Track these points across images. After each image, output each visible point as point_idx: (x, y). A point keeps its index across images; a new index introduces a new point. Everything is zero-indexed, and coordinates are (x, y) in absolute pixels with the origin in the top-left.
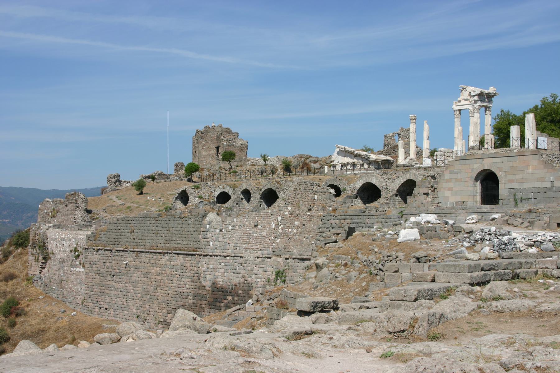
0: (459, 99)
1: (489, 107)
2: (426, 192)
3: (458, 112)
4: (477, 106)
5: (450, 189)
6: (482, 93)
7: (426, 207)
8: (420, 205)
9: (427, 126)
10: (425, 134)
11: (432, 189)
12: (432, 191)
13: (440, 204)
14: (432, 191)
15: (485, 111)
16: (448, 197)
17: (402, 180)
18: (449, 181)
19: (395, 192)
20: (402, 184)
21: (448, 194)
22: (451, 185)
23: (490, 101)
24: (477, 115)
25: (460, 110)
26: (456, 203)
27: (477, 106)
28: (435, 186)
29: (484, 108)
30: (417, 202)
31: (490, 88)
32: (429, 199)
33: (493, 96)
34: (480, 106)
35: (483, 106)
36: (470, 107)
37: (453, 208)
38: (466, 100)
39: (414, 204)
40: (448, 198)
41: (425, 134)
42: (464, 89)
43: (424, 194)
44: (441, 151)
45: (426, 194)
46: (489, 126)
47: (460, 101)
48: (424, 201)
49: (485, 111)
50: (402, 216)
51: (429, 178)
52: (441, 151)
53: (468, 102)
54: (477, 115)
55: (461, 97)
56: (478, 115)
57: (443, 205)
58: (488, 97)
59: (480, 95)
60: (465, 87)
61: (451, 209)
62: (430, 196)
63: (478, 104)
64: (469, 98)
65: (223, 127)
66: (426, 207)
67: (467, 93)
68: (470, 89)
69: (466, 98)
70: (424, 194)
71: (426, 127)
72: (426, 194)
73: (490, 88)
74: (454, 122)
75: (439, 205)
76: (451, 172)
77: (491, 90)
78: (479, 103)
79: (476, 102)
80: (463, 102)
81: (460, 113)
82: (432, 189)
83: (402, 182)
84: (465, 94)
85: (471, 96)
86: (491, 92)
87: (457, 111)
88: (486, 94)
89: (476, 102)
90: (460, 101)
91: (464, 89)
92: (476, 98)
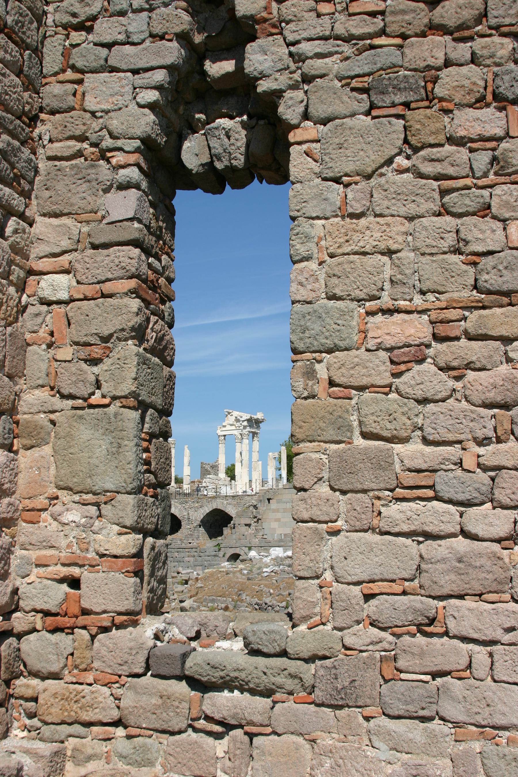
0: (224, 424)
1: (257, 434)
2: (248, 523)
3: (223, 438)
4: (245, 431)
5: (278, 520)
7: (248, 539)
8: (242, 537)
9: (188, 451)
10: (186, 460)
11: (255, 520)
12: (255, 522)
13: (265, 537)
14: (255, 522)
15: (253, 438)
16: (275, 529)
17: (207, 509)
18: (277, 511)
19: (198, 523)
20: (207, 514)
21: (274, 525)
22: (279, 515)
23: (258, 427)
24: (246, 441)
25: (225, 436)
26: (285, 535)
27: (245, 431)
28: (259, 517)
29: (251, 434)
30: (238, 534)
32: (251, 531)
33: (261, 422)
34: (249, 432)
35: (252, 432)
36: (236, 433)
37: (281, 540)
38: (231, 425)
39: (234, 536)
40: (274, 529)
41: (186, 460)
42: (229, 413)
43: (246, 525)
45: (249, 525)
46: (257, 453)
47: (224, 426)
48: (246, 533)
49: (253, 438)
50: (219, 550)
51: (251, 508)
53: (233, 428)
57: (269, 538)
58: (256, 423)
59: (249, 420)
60: (231, 411)
61: (279, 542)
62: (252, 527)
64: (235, 423)
66: (248, 539)
68: (236, 414)
69: (232, 423)
70: (246, 525)
71: (187, 452)
72: (249, 525)
75: (264, 537)
76: (278, 502)
77: (259, 416)
78: (248, 429)
79: (245, 427)
80: (229, 427)
81: (225, 439)
82: (255, 520)
83: (208, 511)
84: (231, 419)
85: (237, 420)
89: (245, 427)
90: (224, 426)
92: (245, 423)
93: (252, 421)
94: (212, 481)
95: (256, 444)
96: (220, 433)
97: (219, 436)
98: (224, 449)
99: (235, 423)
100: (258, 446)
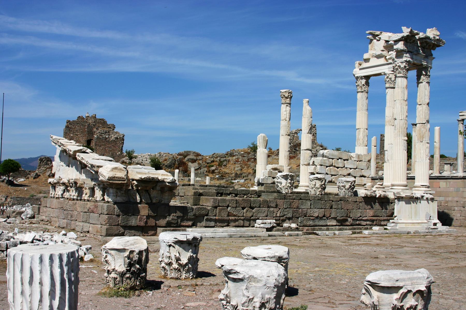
0: (366, 56)
3: (364, 81)
6: (412, 35)
15: (419, 77)
23: (429, 56)
25: (367, 78)
31: (428, 30)
36: (387, 70)
38: (378, 57)
42: (375, 36)
44: (323, 156)
46: (425, 107)
47: (367, 60)
49: (419, 77)
52: (323, 156)
53: (382, 61)
54: (401, 82)
55: (371, 52)
56: (405, 80)
58: (423, 48)
60: (378, 33)
63: (404, 59)
64: (385, 53)
65: (97, 117)
67: (382, 43)
68: (385, 36)
69: (379, 52)
71: (307, 109)
73: (428, 30)
74: (356, 99)
77: (432, 33)
78: (407, 57)
79: (399, 54)
81: (367, 84)
84: (377, 47)
85: (389, 47)
86: (431, 36)
87: (362, 78)
88: (420, 39)
89: (399, 54)
90: (367, 60)
91: (375, 36)
92: (400, 46)
93: (415, 41)
94: (328, 162)
95: (424, 90)
96: (358, 72)
97: (357, 78)
98: (365, 102)
99: (385, 53)
100: (427, 92)
